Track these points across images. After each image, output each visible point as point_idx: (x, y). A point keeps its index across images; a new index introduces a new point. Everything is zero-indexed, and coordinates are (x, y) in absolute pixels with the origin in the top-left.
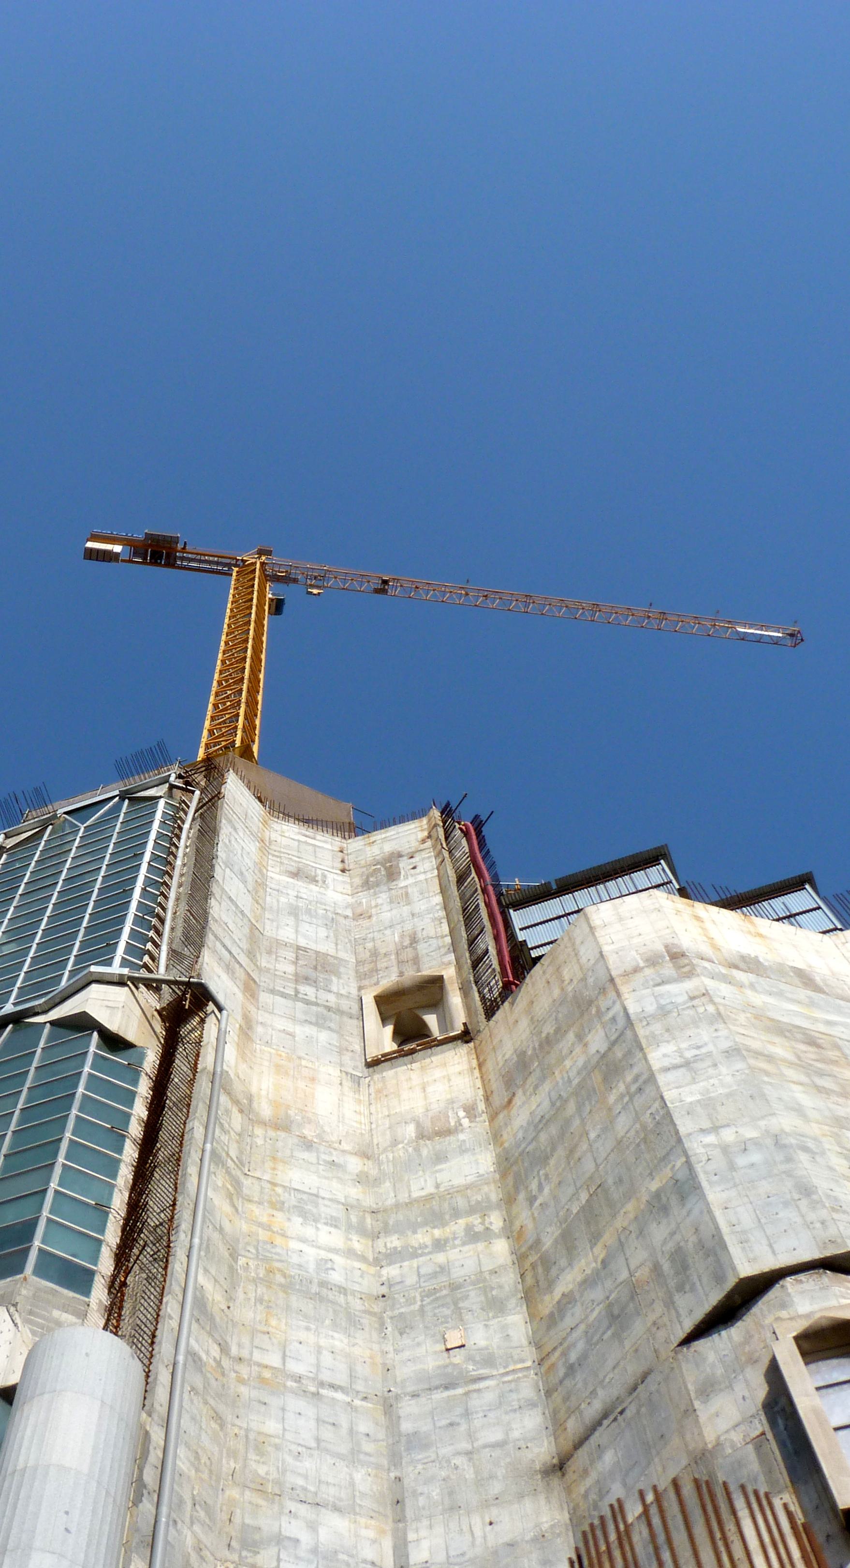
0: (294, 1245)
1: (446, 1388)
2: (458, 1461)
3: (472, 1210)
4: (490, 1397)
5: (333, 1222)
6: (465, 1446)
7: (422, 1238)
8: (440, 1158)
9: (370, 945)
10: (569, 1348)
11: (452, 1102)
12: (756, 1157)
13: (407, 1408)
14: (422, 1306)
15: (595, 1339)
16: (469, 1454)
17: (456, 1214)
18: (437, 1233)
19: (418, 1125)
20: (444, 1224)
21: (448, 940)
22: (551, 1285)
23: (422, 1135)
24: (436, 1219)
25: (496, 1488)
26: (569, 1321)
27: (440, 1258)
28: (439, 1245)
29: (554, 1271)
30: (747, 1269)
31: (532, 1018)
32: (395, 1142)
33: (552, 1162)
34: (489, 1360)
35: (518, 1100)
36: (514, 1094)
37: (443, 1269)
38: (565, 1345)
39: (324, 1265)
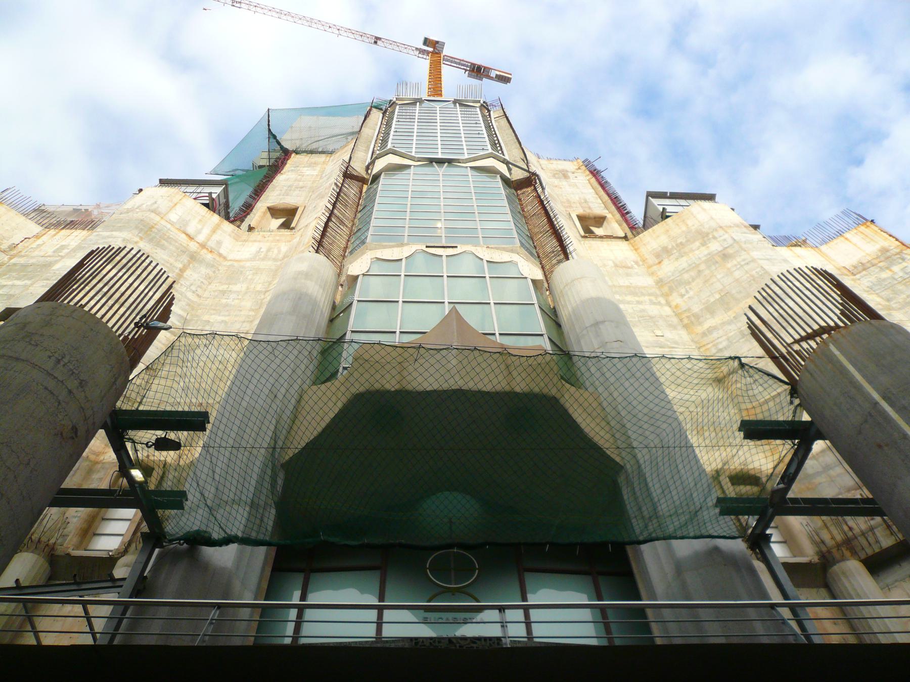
1: (660, 347)
3: (650, 295)
8: (628, 275)
9: (565, 198)
10: (717, 343)
14: (639, 321)
15: (734, 341)
17: (643, 294)
18: (637, 299)
19: (614, 262)
20: (639, 297)
21: (603, 205)
22: (700, 324)
26: (715, 335)
27: (641, 307)
29: (701, 319)
31: (669, 236)
33: (693, 284)
34: (676, 343)
35: (666, 262)
36: (662, 260)
37: (643, 311)
38: (715, 342)
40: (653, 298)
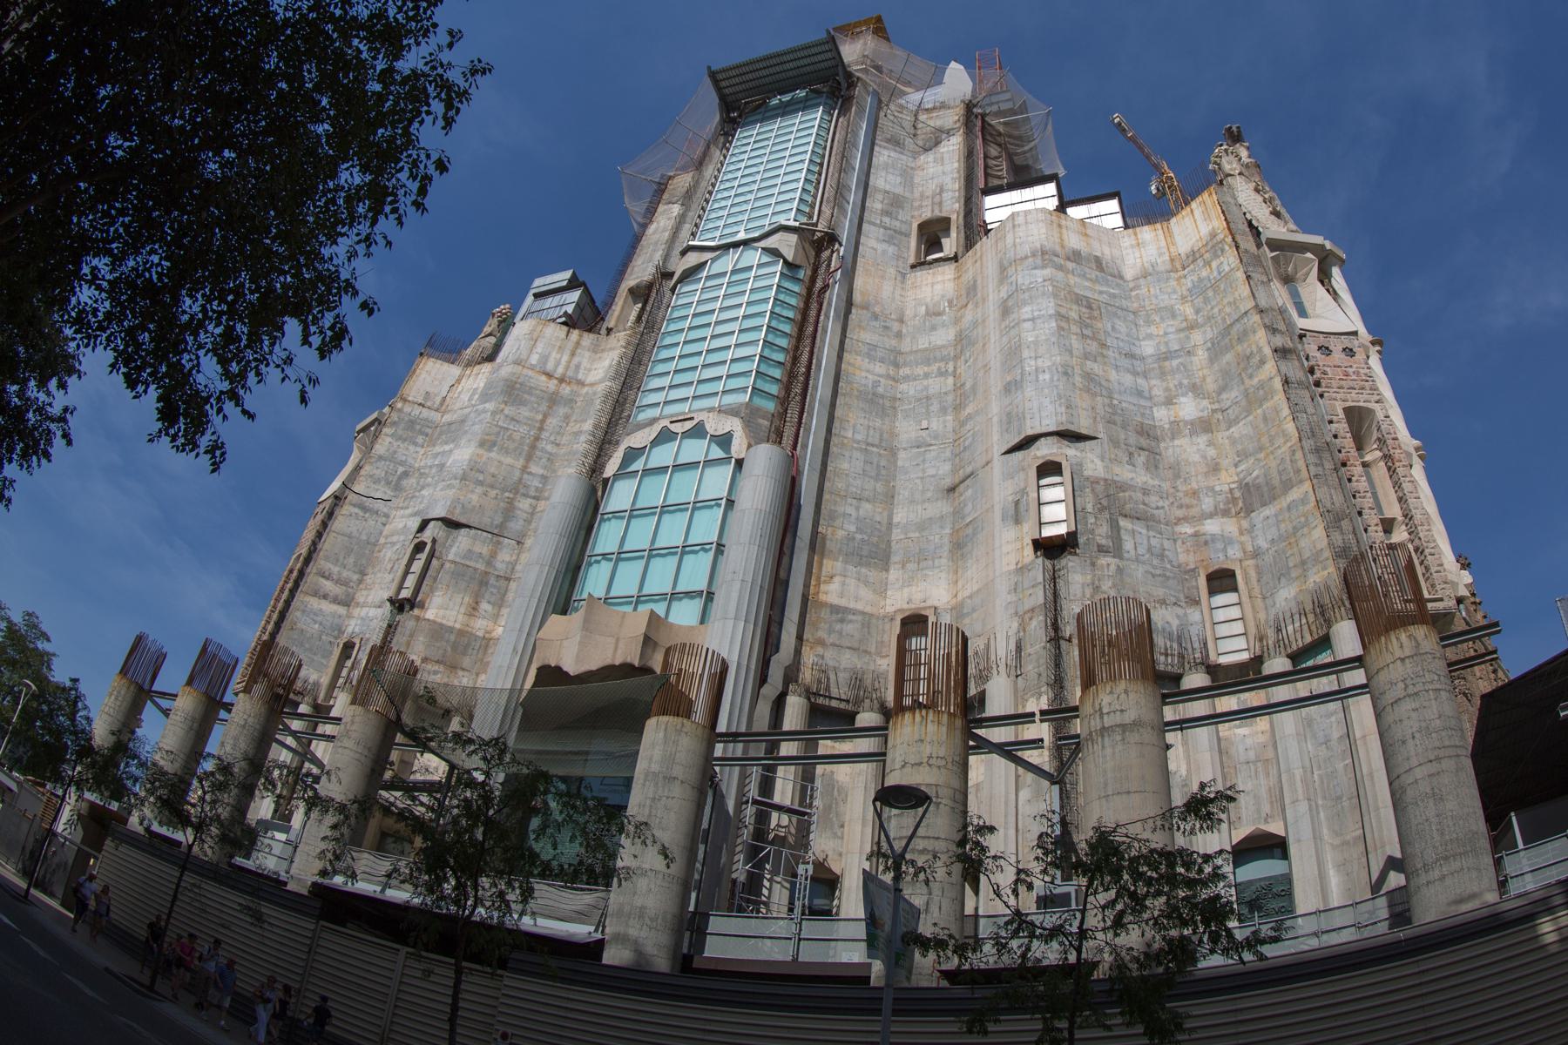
0: (864, 374)
2: (918, 481)
4: (933, 454)
5: (882, 361)
6: (921, 475)
7: (920, 371)
8: (933, 328)
11: (943, 296)
12: (1047, 376)
13: (902, 455)
16: (922, 478)
17: (935, 360)
23: (927, 314)
24: (927, 362)
25: (929, 494)
28: (926, 376)
30: (1030, 432)
32: (915, 316)
34: (936, 437)
37: (926, 388)
39: (876, 384)
40: (942, 365)
